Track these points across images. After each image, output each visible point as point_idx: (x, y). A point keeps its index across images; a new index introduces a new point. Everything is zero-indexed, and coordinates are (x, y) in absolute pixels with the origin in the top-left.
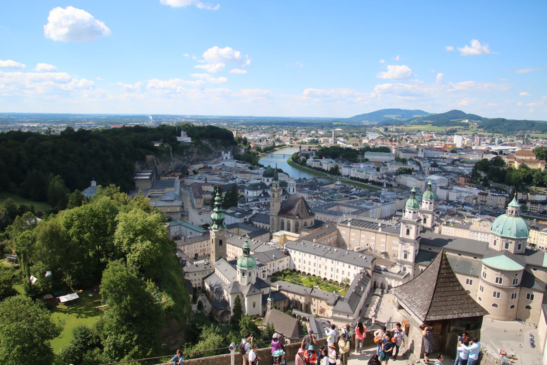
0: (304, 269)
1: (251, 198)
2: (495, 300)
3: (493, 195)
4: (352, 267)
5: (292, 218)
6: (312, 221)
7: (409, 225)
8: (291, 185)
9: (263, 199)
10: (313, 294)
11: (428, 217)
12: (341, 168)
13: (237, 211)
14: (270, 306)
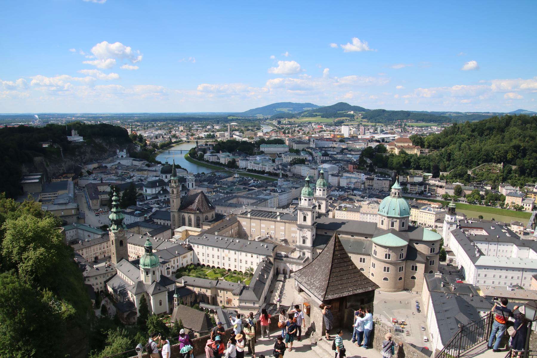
0: (208, 262)
1: (149, 195)
2: (385, 274)
3: (379, 180)
4: (255, 256)
5: (192, 213)
6: (213, 215)
7: (305, 212)
8: (190, 180)
9: (162, 196)
10: (218, 286)
11: (322, 204)
12: (238, 161)
13: (136, 210)
14: (176, 303)
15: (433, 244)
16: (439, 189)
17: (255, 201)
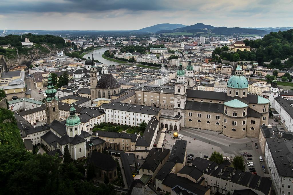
0: (115, 121)
4: (147, 116)
6: (119, 90)
8: (104, 69)
15: (265, 106)
16: (263, 72)
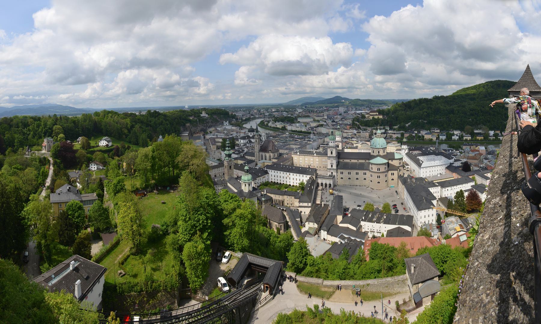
4: (305, 176)
17: (299, 146)
